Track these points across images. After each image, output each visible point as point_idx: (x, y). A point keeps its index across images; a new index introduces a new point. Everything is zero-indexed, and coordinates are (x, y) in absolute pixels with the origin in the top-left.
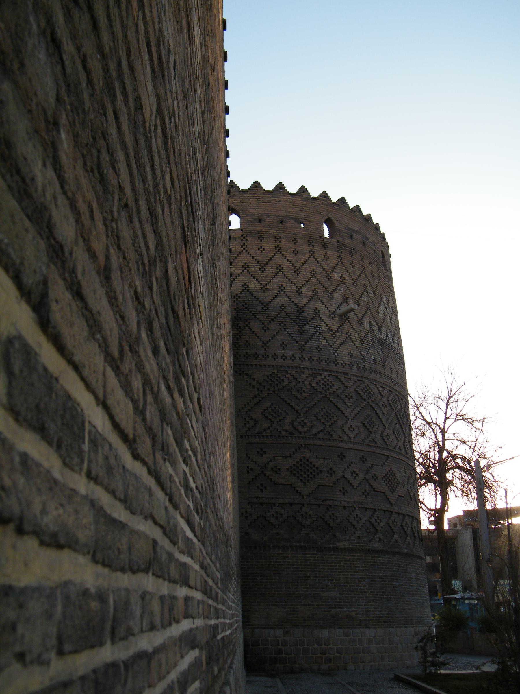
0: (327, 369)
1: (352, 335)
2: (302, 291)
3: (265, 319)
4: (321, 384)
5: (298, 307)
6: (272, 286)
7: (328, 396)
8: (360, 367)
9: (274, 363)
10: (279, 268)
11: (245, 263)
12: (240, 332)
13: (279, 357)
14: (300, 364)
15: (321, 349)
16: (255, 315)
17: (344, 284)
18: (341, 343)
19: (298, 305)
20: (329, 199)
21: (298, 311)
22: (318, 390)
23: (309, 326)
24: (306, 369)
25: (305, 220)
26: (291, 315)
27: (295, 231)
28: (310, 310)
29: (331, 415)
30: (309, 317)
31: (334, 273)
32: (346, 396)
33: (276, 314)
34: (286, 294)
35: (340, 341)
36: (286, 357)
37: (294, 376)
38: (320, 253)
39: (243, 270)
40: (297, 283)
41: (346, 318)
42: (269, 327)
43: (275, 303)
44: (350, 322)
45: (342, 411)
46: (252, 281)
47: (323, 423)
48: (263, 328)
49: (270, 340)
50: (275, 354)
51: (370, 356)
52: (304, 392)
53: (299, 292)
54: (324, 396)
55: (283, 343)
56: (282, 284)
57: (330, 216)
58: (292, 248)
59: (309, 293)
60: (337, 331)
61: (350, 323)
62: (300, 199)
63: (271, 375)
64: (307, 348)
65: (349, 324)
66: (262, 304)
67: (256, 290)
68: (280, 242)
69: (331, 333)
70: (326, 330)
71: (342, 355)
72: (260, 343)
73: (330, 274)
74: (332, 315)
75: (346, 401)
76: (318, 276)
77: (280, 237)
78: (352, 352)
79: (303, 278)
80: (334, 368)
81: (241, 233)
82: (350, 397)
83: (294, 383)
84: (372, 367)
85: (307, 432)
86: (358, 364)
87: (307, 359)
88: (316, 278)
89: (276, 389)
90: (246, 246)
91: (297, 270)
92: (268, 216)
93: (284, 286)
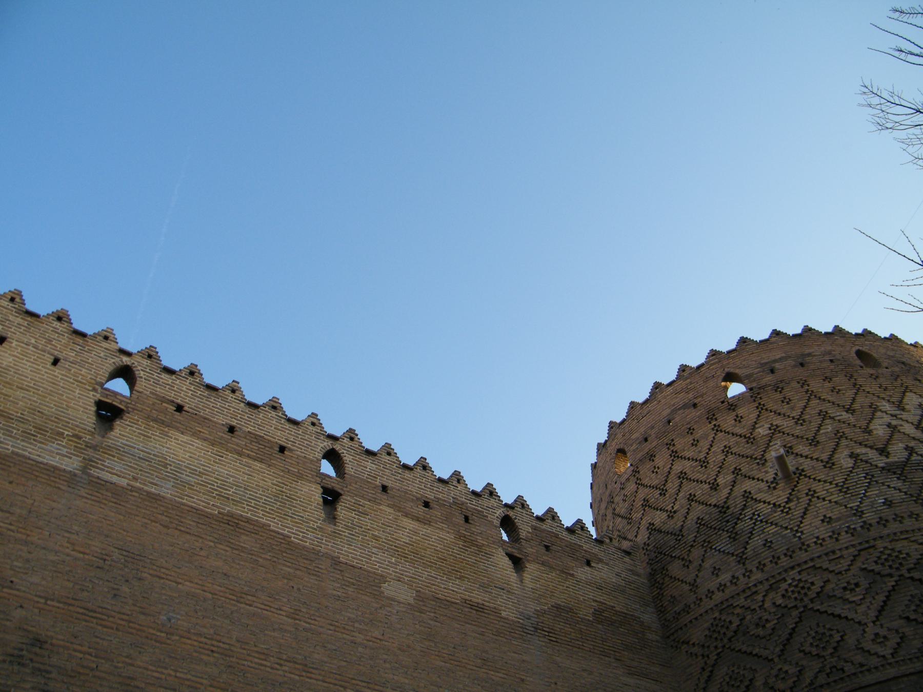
0: (792, 564)
1: (817, 491)
2: (718, 485)
3: (683, 552)
4: (790, 594)
5: (718, 507)
7: (810, 606)
8: (854, 529)
10: (682, 476)
11: (644, 499)
12: (660, 588)
14: (747, 584)
15: (771, 542)
17: (780, 432)
18: (802, 514)
19: (717, 504)
20: (720, 353)
21: (720, 512)
22: (789, 606)
23: (742, 522)
24: (758, 584)
26: (712, 524)
28: (736, 500)
29: (828, 634)
30: (737, 510)
31: (757, 430)
32: (845, 589)
33: (693, 535)
34: (699, 502)
35: (798, 513)
36: (725, 585)
37: (743, 606)
38: (727, 421)
39: (644, 510)
40: (708, 479)
41: (798, 475)
43: (688, 522)
44: (808, 475)
45: (846, 618)
47: (817, 655)
48: (684, 565)
50: (709, 590)
51: (871, 502)
52: (767, 620)
53: (714, 487)
54: (802, 609)
55: (715, 568)
56: (690, 492)
57: (726, 370)
59: (728, 479)
60: (789, 500)
61: (809, 477)
63: (712, 624)
64: (750, 553)
65: (807, 479)
66: (675, 534)
68: (674, 445)
69: (779, 510)
70: (770, 510)
71: (811, 529)
72: (687, 587)
73: (752, 434)
74: (773, 485)
75: (848, 595)
76: (734, 450)
77: (673, 440)
78: (828, 516)
79: (715, 466)
80: (802, 556)
81: (632, 468)
82: (853, 586)
83: (748, 617)
84: (882, 515)
85: (795, 686)
86: (848, 527)
87: (754, 570)
88: (732, 454)
89: (726, 640)
91: (704, 462)
92: (652, 427)
93: (692, 494)
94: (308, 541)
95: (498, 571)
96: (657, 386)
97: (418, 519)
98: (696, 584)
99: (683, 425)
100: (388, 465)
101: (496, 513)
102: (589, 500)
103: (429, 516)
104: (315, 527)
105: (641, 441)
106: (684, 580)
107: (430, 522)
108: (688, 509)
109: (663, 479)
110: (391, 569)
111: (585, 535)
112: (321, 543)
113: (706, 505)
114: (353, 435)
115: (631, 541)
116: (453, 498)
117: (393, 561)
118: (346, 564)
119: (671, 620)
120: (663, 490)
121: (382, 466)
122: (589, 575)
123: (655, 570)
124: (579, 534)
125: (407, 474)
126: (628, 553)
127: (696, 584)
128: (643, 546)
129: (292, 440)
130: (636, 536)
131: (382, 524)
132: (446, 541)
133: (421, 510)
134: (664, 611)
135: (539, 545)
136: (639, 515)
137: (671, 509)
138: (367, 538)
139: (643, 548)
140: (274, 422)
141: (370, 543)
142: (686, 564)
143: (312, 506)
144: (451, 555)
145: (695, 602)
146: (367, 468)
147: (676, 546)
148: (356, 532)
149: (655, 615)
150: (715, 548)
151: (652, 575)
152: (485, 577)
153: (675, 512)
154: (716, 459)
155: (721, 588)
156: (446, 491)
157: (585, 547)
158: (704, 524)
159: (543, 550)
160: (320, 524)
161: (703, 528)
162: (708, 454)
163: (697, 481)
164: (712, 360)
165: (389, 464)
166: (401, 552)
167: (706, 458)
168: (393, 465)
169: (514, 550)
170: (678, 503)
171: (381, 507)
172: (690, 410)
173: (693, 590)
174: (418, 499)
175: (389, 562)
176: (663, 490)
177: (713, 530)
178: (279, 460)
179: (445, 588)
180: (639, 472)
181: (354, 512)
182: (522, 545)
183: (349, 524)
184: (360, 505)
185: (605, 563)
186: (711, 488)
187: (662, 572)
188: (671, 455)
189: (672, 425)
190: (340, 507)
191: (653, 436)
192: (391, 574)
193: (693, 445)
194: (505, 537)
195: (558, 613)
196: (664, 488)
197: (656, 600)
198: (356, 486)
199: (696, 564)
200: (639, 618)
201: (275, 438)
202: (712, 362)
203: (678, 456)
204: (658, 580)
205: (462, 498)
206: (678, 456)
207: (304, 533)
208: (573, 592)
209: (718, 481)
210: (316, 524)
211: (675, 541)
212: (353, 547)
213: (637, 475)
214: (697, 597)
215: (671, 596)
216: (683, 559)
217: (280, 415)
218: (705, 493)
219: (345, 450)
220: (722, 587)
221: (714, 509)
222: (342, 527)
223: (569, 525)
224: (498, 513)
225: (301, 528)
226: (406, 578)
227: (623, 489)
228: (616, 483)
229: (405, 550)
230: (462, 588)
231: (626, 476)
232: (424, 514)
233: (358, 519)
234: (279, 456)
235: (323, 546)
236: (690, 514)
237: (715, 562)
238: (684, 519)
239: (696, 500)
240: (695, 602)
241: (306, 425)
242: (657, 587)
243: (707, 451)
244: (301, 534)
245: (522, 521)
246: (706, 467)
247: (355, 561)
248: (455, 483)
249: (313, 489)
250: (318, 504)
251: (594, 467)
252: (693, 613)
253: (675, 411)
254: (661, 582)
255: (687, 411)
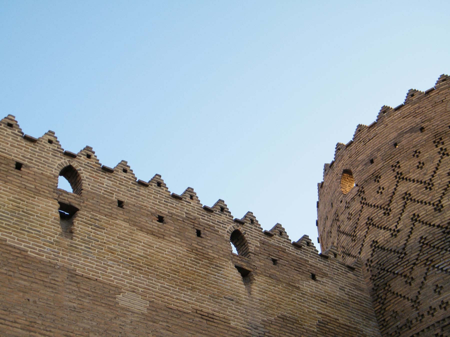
2: (442, 206)
3: (405, 270)
5: (442, 227)
6: (403, 224)
9: (433, 320)
10: (407, 197)
11: (368, 218)
12: (383, 303)
13: (438, 308)
16: (393, 271)
19: (441, 225)
21: (444, 232)
25: (422, 122)
27: (414, 143)
33: (416, 254)
34: (423, 222)
39: (368, 228)
40: (432, 200)
42: (413, 275)
43: (412, 241)
46: (379, 233)
48: (406, 282)
49: (419, 292)
55: (437, 286)
56: (414, 212)
58: (414, 165)
62: (410, 106)
66: (398, 252)
67: (387, 240)
68: (399, 167)
77: (398, 162)
79: (439, 188)
81: (357, 188)
90: (365, 198)
91: (429, 184)
92: (379, 150)
94: (45, 254)
95: (229, 283)
96: (385, 110)
97: (153, 234)
98: (418, 301)
99: (409, 148)
100: (124, 182)
101: (226, 228)
102: (315, 217)
103: (163, 231)
104: (52, 241)
105: (367, 163)
106: (406, 296)
107: (164, 236)
108: (412, 228)
109: (388, 199)
110: (126, 280)
111: (311, 250)
112: (58, 256)
113: (430, 225)
114: (90, 153)
115: (354, 257)
116: (186, 213)
117: (128, 273)
118: (82, 276)
119: (393, 334)
120: (387, 209)
121: (118, 182)
122: (314, 288)
123: (378, 286)
124: (304, 249)
125: (143, 190)
126: (351, 269)
127: (418, 301)
128: (366, 262)
129: (29, 157)
130: (360, 253)
131: (118, 237)
132: (178, 254)
133: (156, 224)
134: (386, 325)
135: (267, 259)
136: (363, 233)
137: (395, 228)
138: (103, 251)
139: (366, 264)
140: (10, 140)
141: (106, 256)
142: (409, 281)
143: (49, 220)
144: (184, 267)
145: (416, 318)
146: (103, 184)
147: (399, 264)
148: (92, 246)
149: (377, 329)
150: (438, 267)
151: (375, 290)
152: (215, 288)
153: (398, 231)
154: (442, 181)
155: (443, 306)
156: (180, 207)
157: (311, 261)
158: (427, 244)
159: (271, 264)
160: (57, 238)
161: (425, 248)
162: (433, 176)
163: (421, 202)
164: (442, 85)
165: (125, 180)
166: (136, 264)
167: (431, 180)
168: (129, 182)
169: (243, 263)
170: (401, 223)
171: (117, 222)
172: (417, 133)
173: (415, 306)
174: (152, 214)
175: (124, 274)
176: (387, 209)
177: (435, 249)
178: (15, 177)
179: (177, 299)
180: (364, 192)
181: (90, 227)
182: (250, 258)
183: (86, 238)
184: (96, 219)
185: (329, 277)
186: (435, 209)
187: (384, 288)
188: (396, 177)
189: (398, 148)
190: (77, 221)
191: (379, 158)
192: (125, 286)
193: (418, 167)
194: (235, 250)
195: (285, 324)
196: (389, 208)
197: (378, 314)
198: (93, 202)
199: (418, 281)
200: (362, 331)
201: (11, 155)
202: (442, 87)
203: (403, 178)
204: (381, 295)
205: (195, 213)
206: (403, 178)
207: (41, 247)
208: (299, 304)
209: (442, 203)
210: (52, 238)
211: (397, 258)
212: (89, 260)
213: (362, 195)
214: (418, 313)
215: (393, 311)
216: (405, 276)
217: (16, 132)
218: (429, 214)
219: (82, 167)
220: (445, 305)
221: (437, 230)
222: (79, 241)
223: (296, 241)
224: (228, 228)
225: (38, 242)
226: (140, 289)
227: (348, 207)
228: (341, 202)
229: (139, 262)
230: (194, 299)
231: (351, 196)
232: (158, 229)
233: (94, 233)
234: (15, 173)
235: (60, 259)
236: (413, 234)
237: (438, 280)
238: (407, 238)
239: (419, 220)
240: (416, 318)
241: (43, 143)
242: (379, 302)
243: (433, 173)
244: (38, 248)
245: (251, 236)
246: (430, 189)
247: (91, 273)
248: (188, 199)
249: (50, 204)
250: (55, 219)
251: (321, 186)
252: (415, 328)
253: (401, 135)
254: (383, 298)
255: (414, 135)
